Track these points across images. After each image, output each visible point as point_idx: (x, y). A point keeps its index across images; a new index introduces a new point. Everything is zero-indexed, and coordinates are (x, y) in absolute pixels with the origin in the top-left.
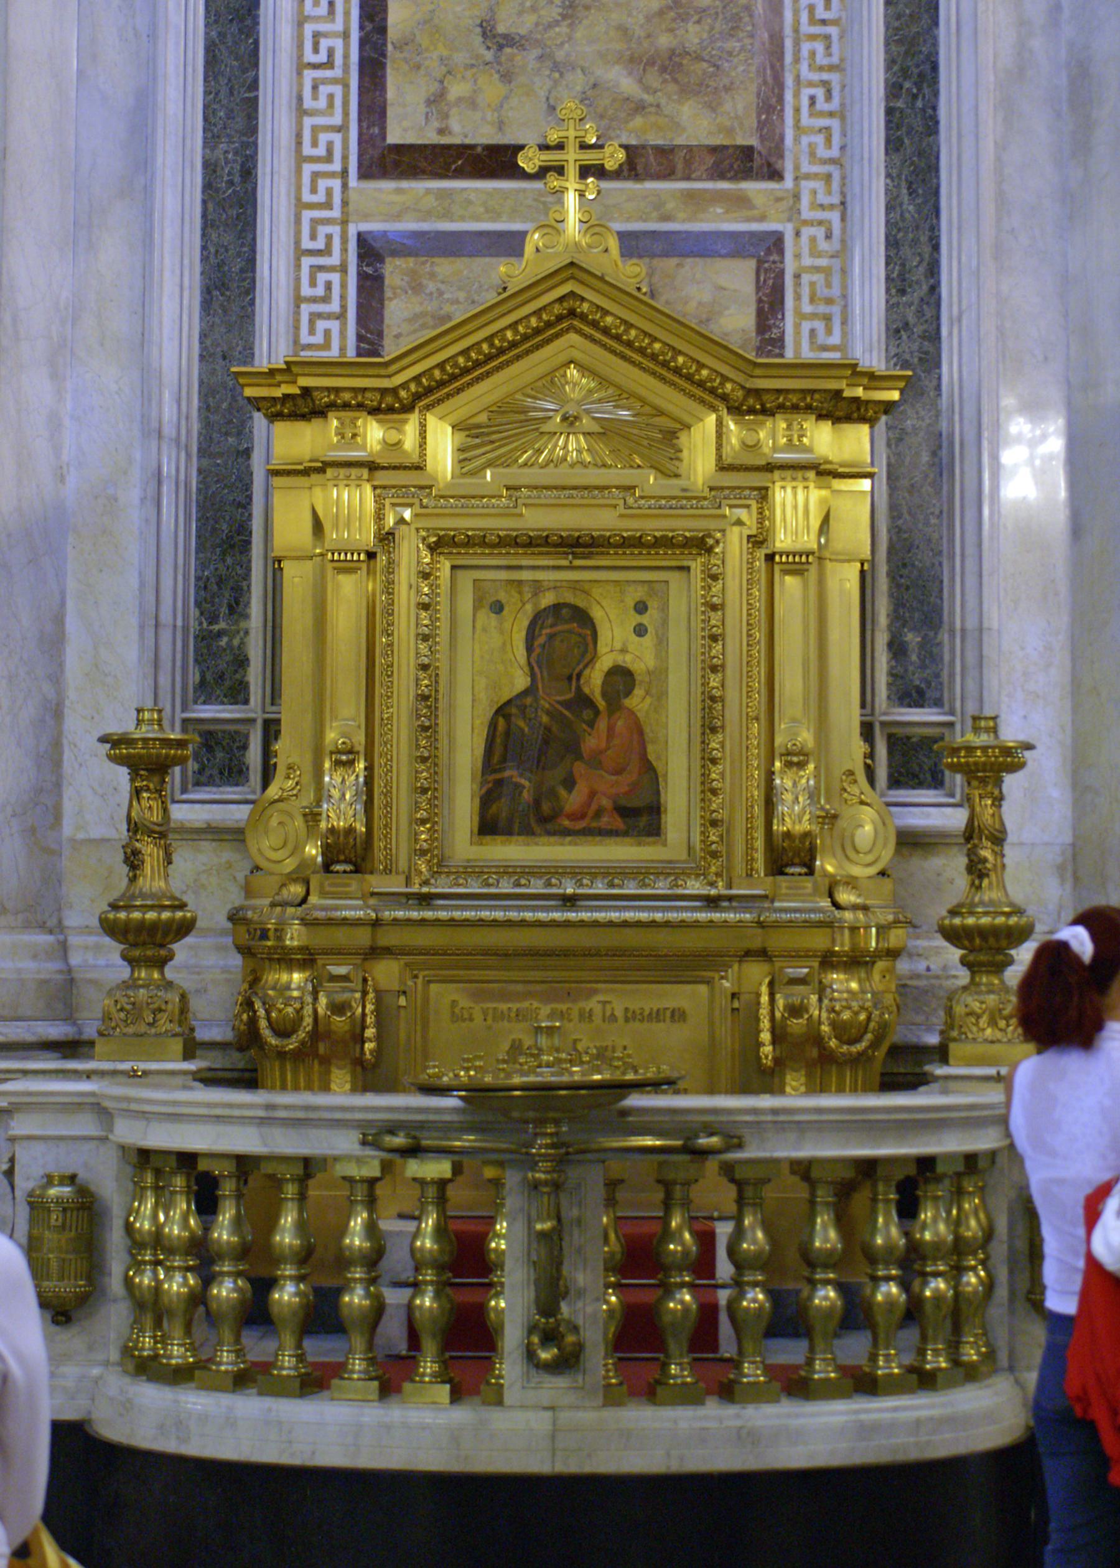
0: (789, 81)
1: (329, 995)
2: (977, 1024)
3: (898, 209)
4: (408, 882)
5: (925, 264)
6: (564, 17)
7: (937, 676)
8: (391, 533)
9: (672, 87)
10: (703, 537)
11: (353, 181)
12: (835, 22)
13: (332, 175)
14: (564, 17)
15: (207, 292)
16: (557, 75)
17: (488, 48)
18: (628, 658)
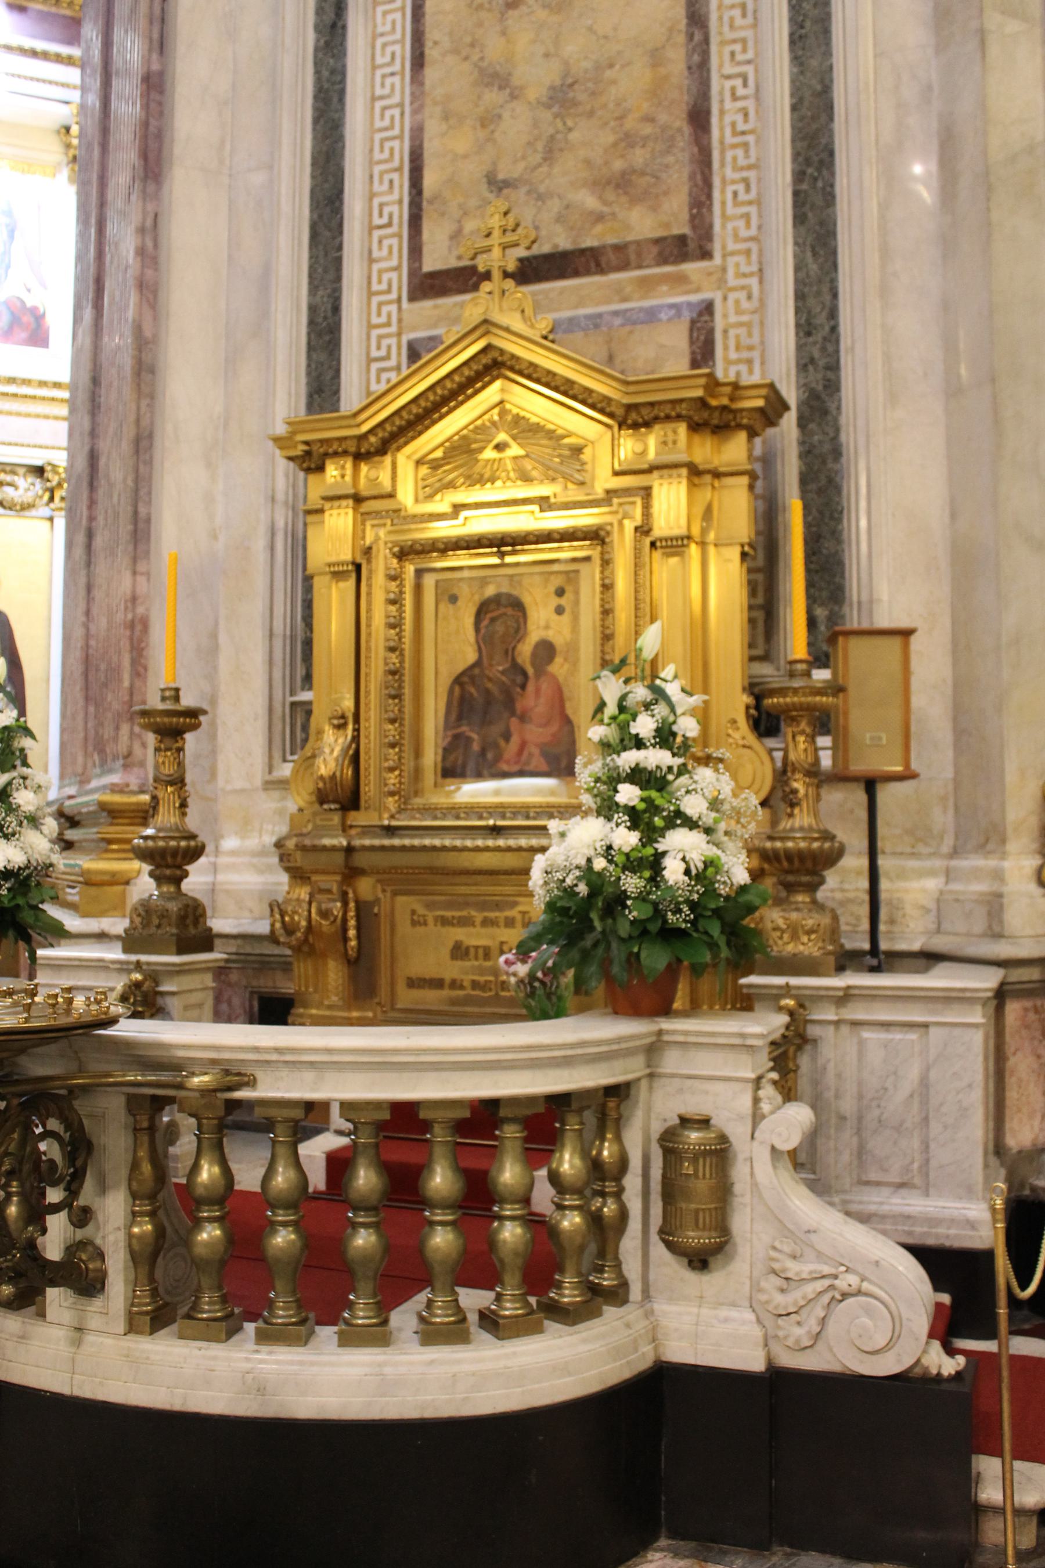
0: (716, 181)
1: (319, 904)
2: (781, 938)
6: (545, 159)
9: (624, 199)
12: (751, 132)
15: (310, 396)
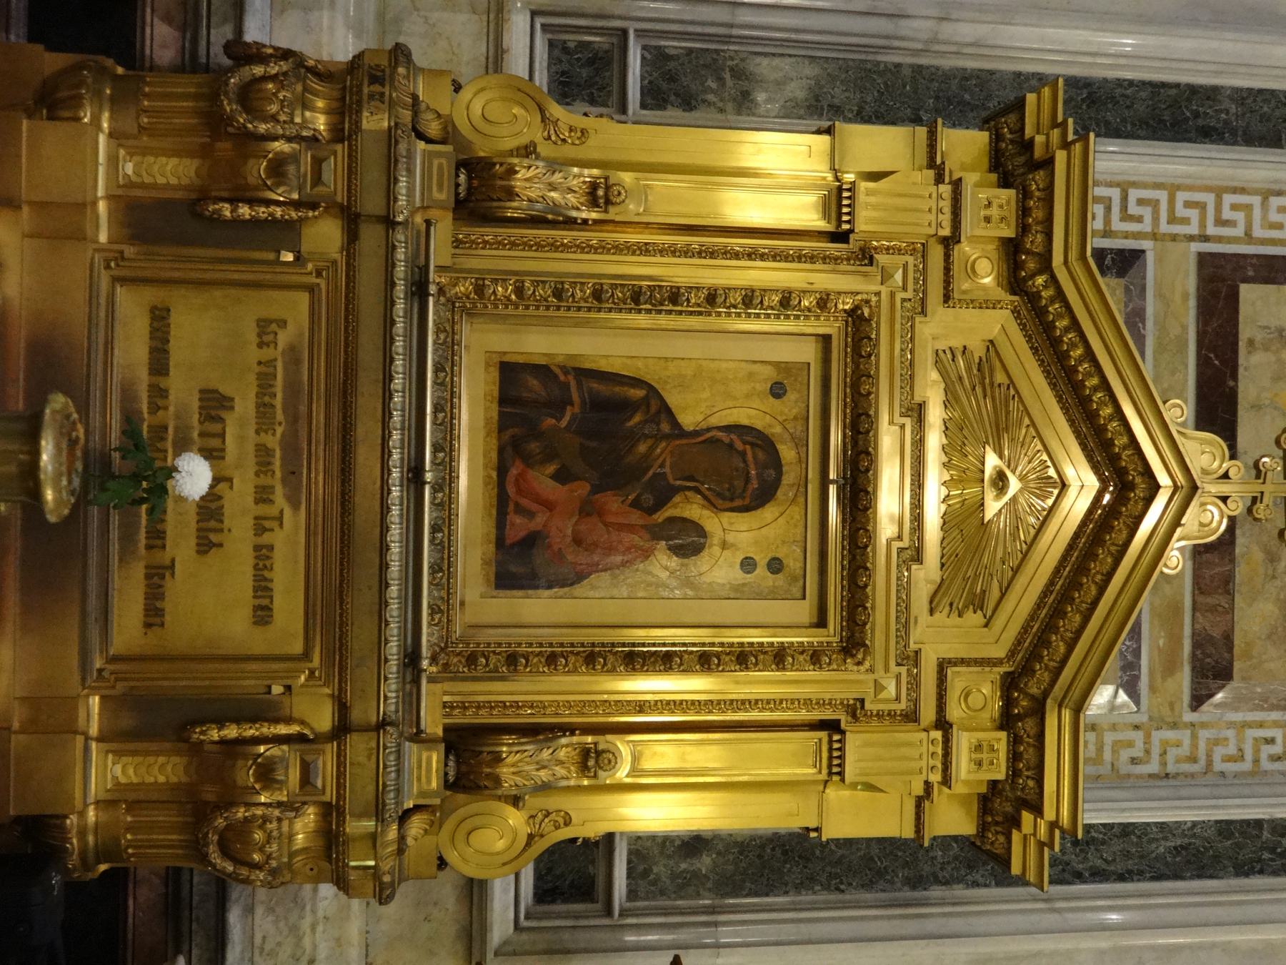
1: (295, 158)
3: (1161, 835)
4: (441, 269)
5: (1104, 866)
7: (662, 893)
8: (871, 259)
10: (865, 645)
11: (1196, 247)
13: (1203, 224)
18: (716, 550)
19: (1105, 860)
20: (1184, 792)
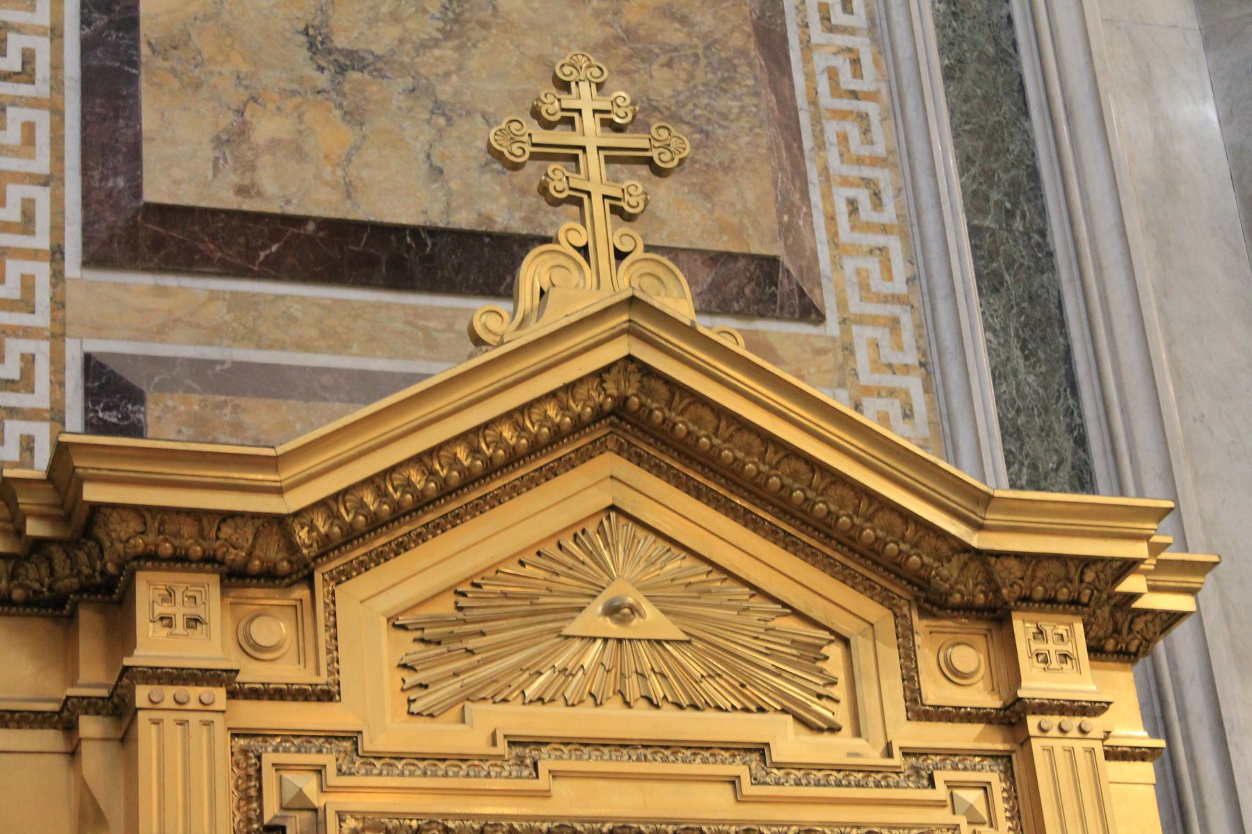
0: (813, 174)
3: (1011, 379)
5: (1067, 467)
12: (872, 97)
13: (34, 255)
14: (447, 35)
16: (442, 121)
17: (321, 69)
19: (1060, 464)
20: (948, 339)
